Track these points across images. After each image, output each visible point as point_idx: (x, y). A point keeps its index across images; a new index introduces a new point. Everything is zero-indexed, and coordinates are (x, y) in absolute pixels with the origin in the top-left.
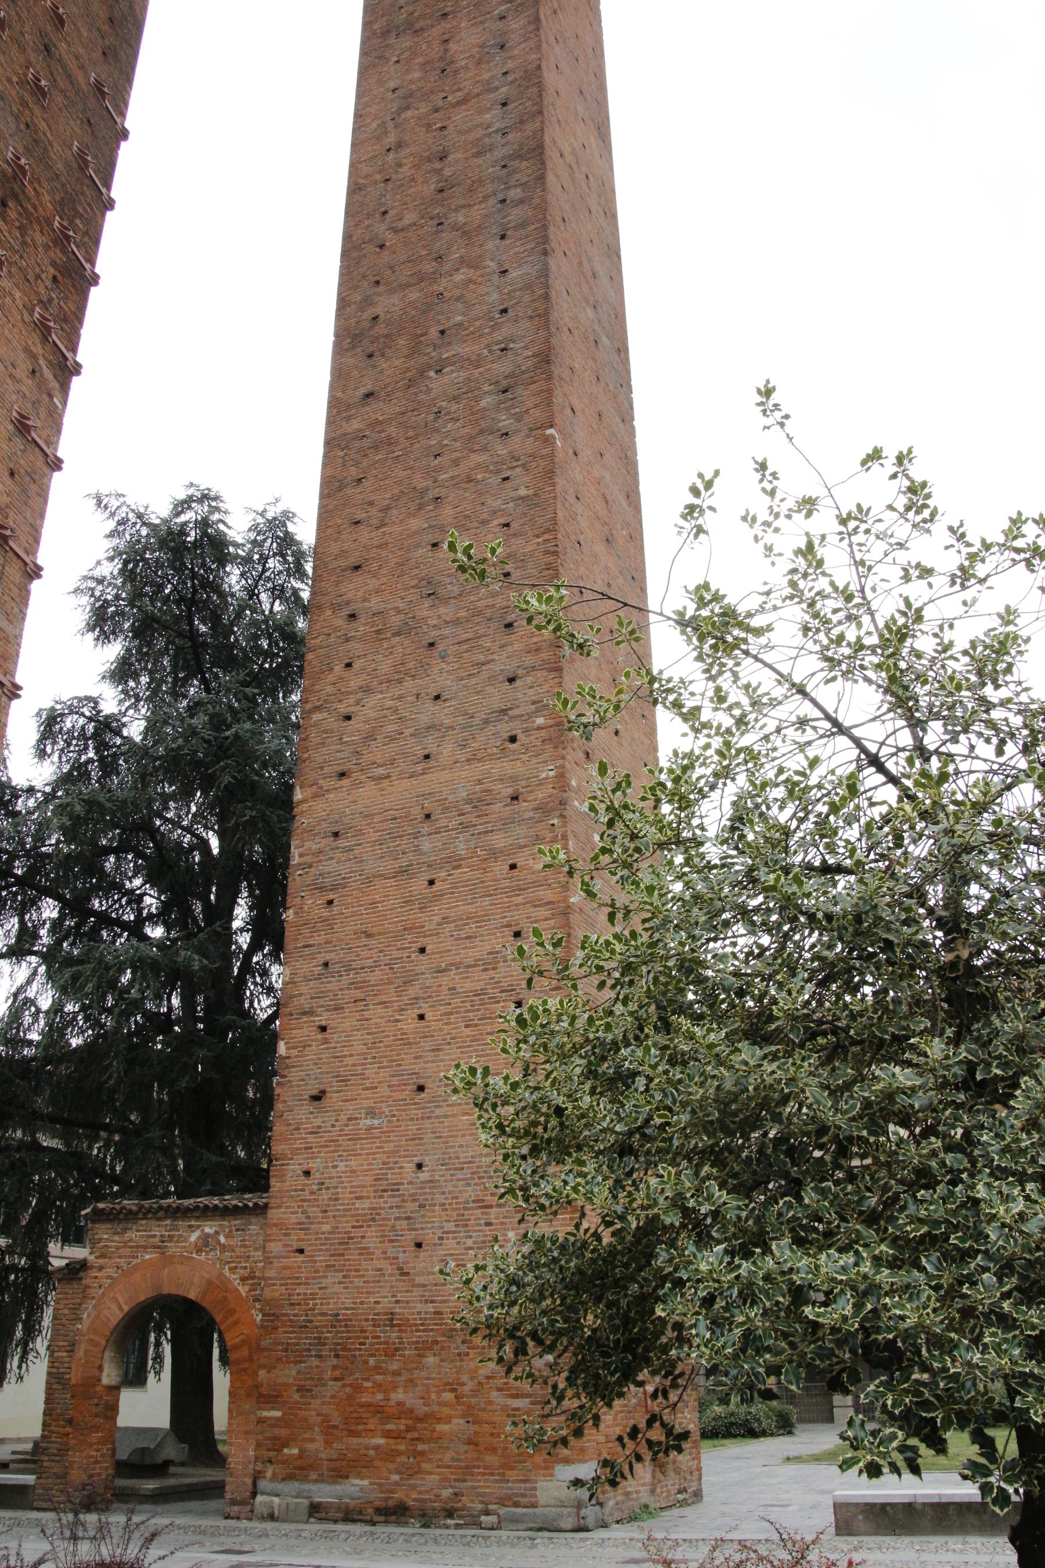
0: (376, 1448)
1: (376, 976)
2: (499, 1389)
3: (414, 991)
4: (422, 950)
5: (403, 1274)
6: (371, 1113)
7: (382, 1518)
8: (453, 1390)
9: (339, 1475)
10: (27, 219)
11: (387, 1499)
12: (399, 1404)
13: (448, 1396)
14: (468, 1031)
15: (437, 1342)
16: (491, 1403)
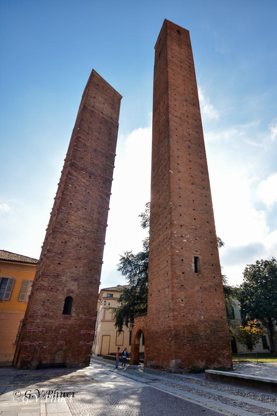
0: (156, 355)
1: (155, 273)
2: (166, 345)
3: (158, 275)
4: (159, 268)
5: (158, 324)
6: (155, 296)
7: (156, 368)
8: (162, 345)
9: (153, 360)
10: (96, 176)
11: (157, 364)
12: (158, 347)
13: (162, 346)
14: (163, 280)
15: (161, 336)
16: (166, 347)
